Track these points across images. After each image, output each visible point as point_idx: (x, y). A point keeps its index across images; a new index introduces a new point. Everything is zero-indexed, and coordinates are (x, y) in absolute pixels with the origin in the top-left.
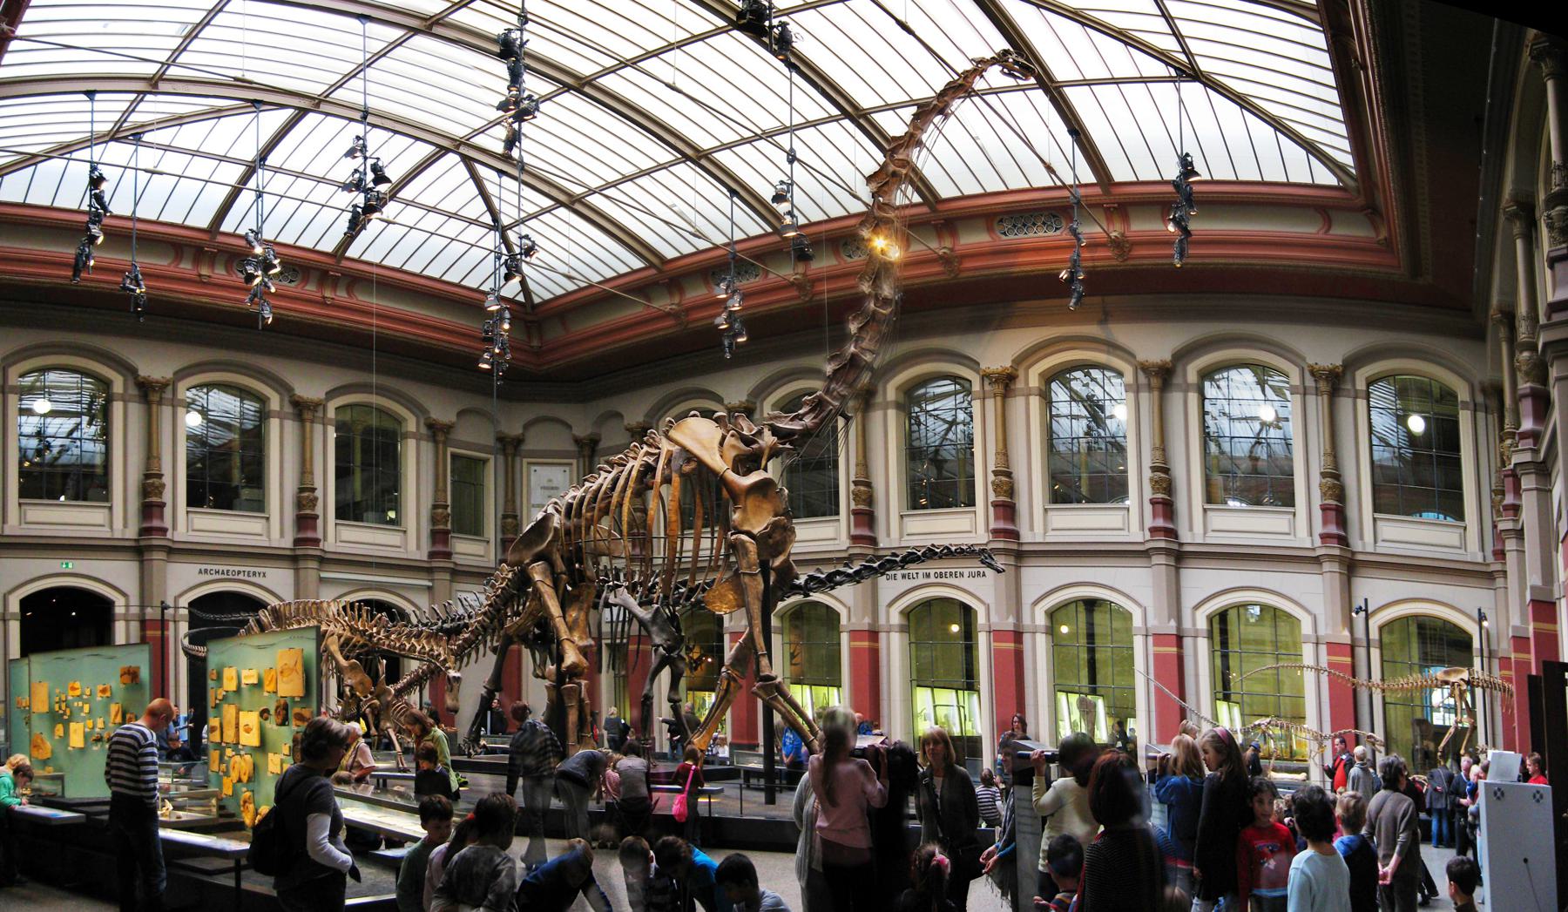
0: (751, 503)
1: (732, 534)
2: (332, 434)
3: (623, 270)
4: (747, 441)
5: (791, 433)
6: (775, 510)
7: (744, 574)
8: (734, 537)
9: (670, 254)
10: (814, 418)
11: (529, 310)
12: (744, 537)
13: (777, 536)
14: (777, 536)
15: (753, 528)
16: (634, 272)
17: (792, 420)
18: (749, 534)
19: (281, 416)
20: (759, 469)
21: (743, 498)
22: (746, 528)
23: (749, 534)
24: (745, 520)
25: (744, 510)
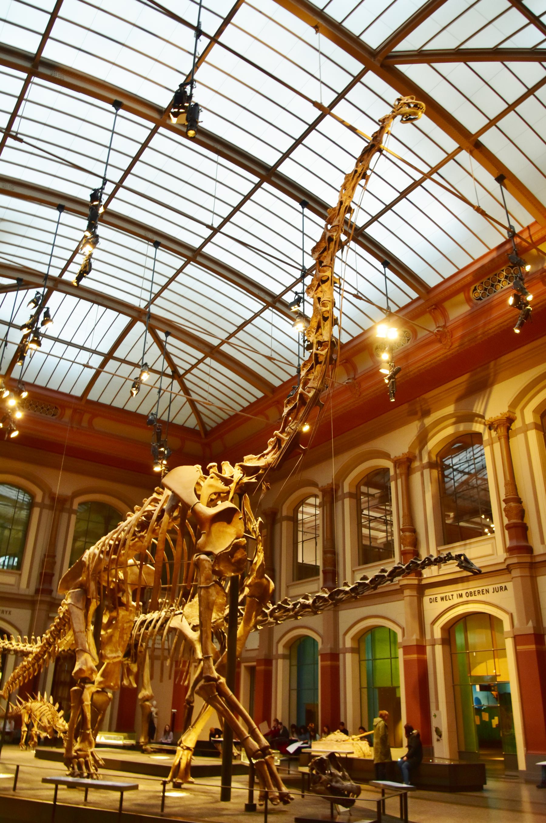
0: (216, 527)
1: (197, 556)
2: (74, 517)
3: (253, 400)
4: (227, 482)
5: (257, 469)
6: (237, 534)
7: (201, 588)
8: (198, 557)
9: (277, 383)
10: (275, 454)
11: (203, 435)
12: (203, 557)
13: (238, 555)
14: (238, 555)
15: (216, 550)
16: (259, 400)
17: (259, 458)
18: (209, 554)
19: (42, 506)
20: (227, 500)
21: (207, 525)
22: (208, 549)
23: (209, 554)
24: (206, 543)
25: (209, 534)
